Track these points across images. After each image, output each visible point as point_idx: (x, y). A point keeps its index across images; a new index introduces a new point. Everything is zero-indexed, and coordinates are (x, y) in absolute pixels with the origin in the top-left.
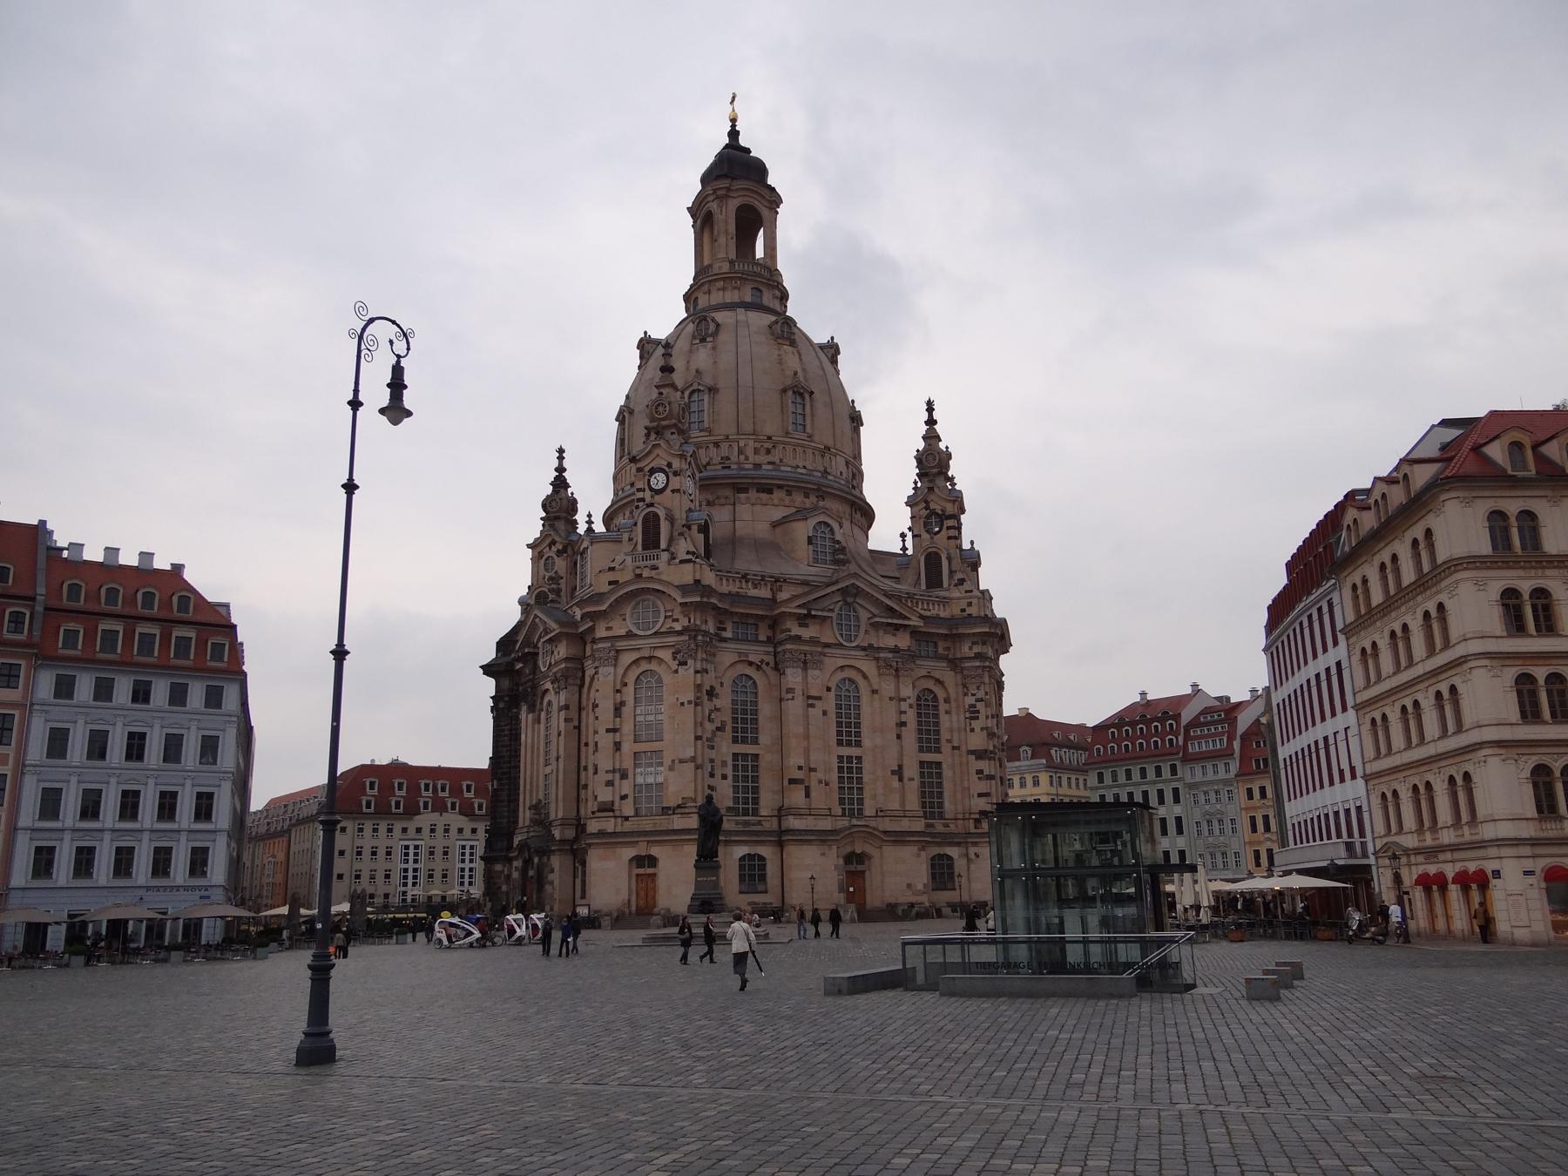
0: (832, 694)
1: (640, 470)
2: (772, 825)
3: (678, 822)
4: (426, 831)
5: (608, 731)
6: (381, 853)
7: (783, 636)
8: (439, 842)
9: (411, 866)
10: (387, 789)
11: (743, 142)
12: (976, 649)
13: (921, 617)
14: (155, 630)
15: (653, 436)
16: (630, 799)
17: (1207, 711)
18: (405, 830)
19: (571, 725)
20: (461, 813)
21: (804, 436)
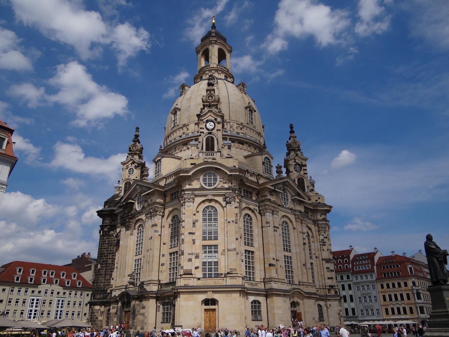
0: (280, 227)
3: (229, 282)
4: (43, 293)
5: (190, 233)
6: (21, 302)
7: (264, 198)
8: (48, 298)
9: (34, 309)
12: (323, 217)
13: (309, 199)
15: (206, 109)
16: (200, 269)
17: (356, 256)
18: (33, 292)
19: (157, 234)
20: (59, 285)
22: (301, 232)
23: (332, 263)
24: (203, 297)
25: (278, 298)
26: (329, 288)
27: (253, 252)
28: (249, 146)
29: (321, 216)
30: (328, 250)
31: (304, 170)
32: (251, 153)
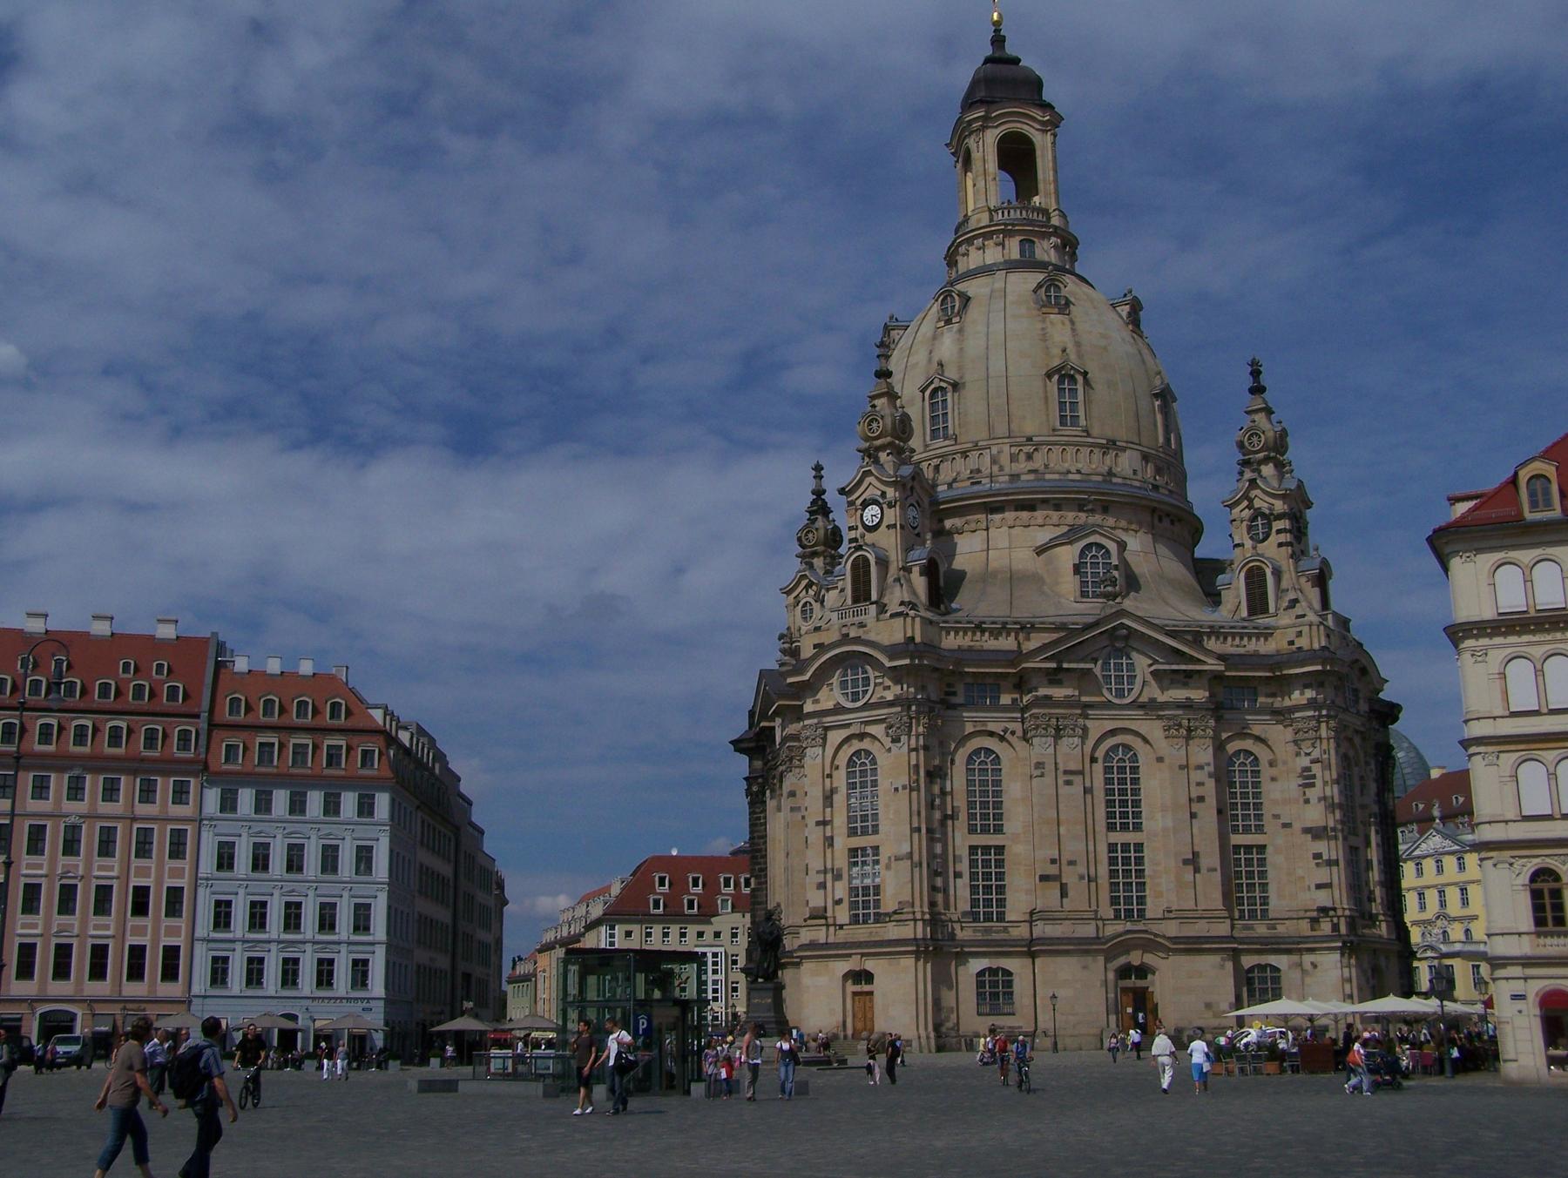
0: (1098, 768)
1: (851, 504)
2: (1021, 932)
3: (893, 931)
4: (725, 936)
5: (818, 823)
10: (678, 886)
11: (1010, 49)
12: (1310, 694)
13: (1221, 657)
14: (306, 740)
16: (846, 904)
18: (700, 934)
21: (1076, 431)
22: (1181, 767)
23: (1329, 838)
24: (843, 967)
25: (1060, 960)
26: (1315, 914)
27: (1000, 849)
28: (1057, 507)
29: (1302, 694)
30: (1320, 800)
31: (1279, 532)
32: (1066, 529)
